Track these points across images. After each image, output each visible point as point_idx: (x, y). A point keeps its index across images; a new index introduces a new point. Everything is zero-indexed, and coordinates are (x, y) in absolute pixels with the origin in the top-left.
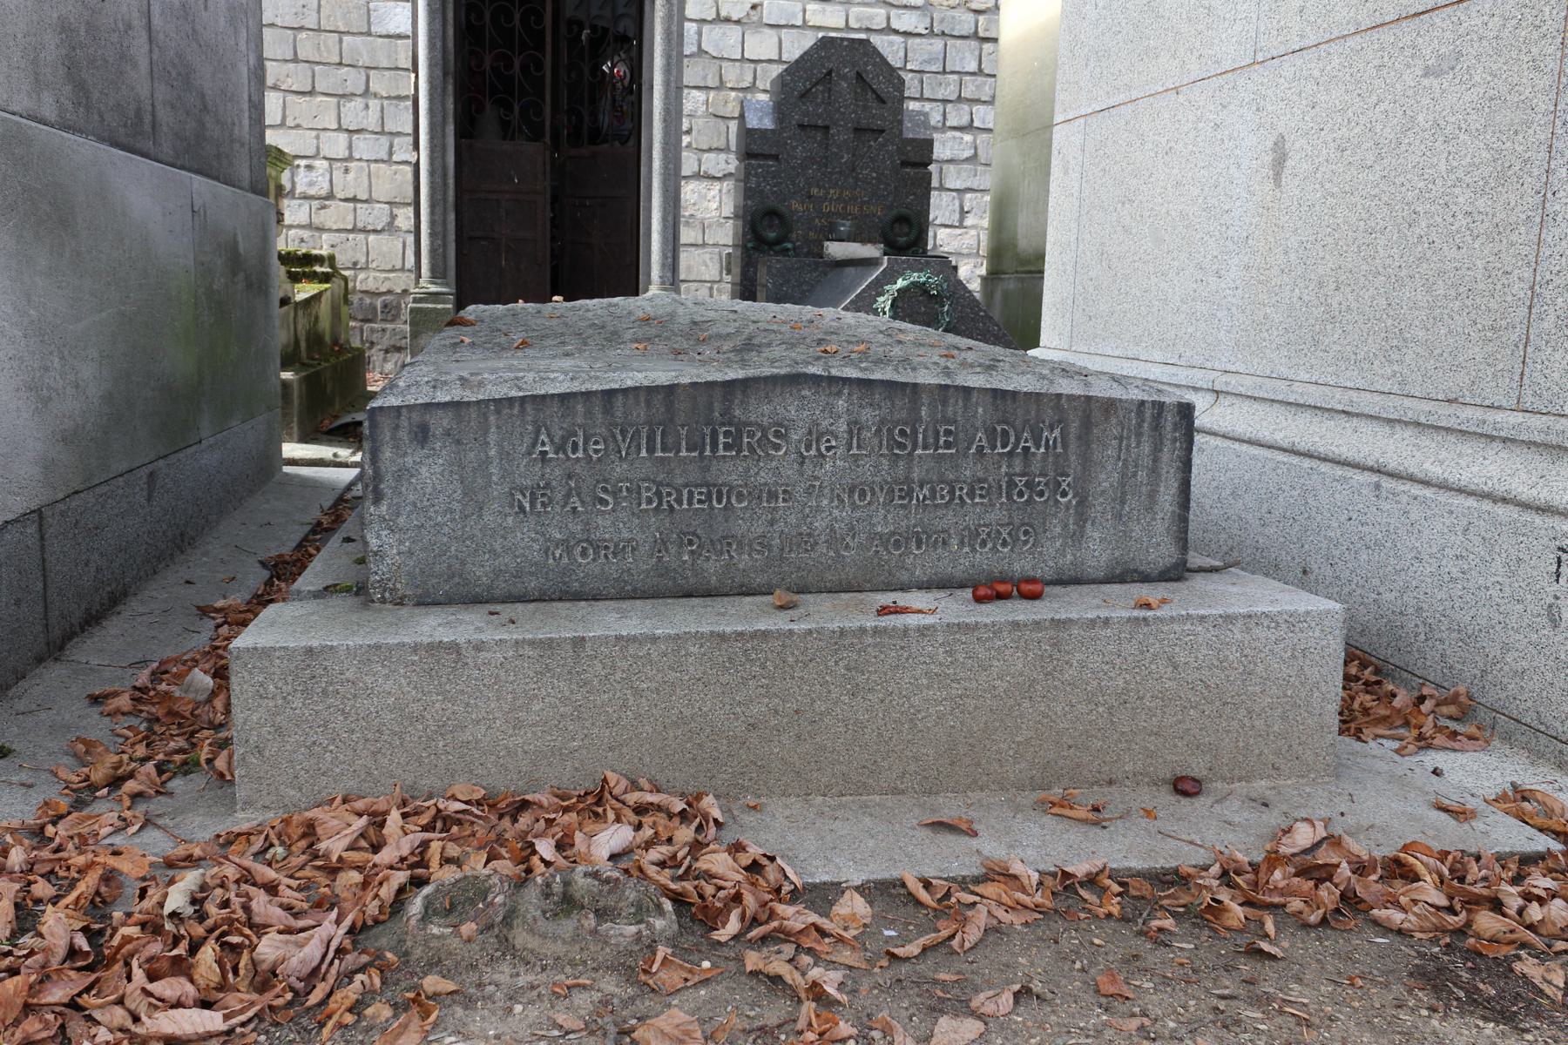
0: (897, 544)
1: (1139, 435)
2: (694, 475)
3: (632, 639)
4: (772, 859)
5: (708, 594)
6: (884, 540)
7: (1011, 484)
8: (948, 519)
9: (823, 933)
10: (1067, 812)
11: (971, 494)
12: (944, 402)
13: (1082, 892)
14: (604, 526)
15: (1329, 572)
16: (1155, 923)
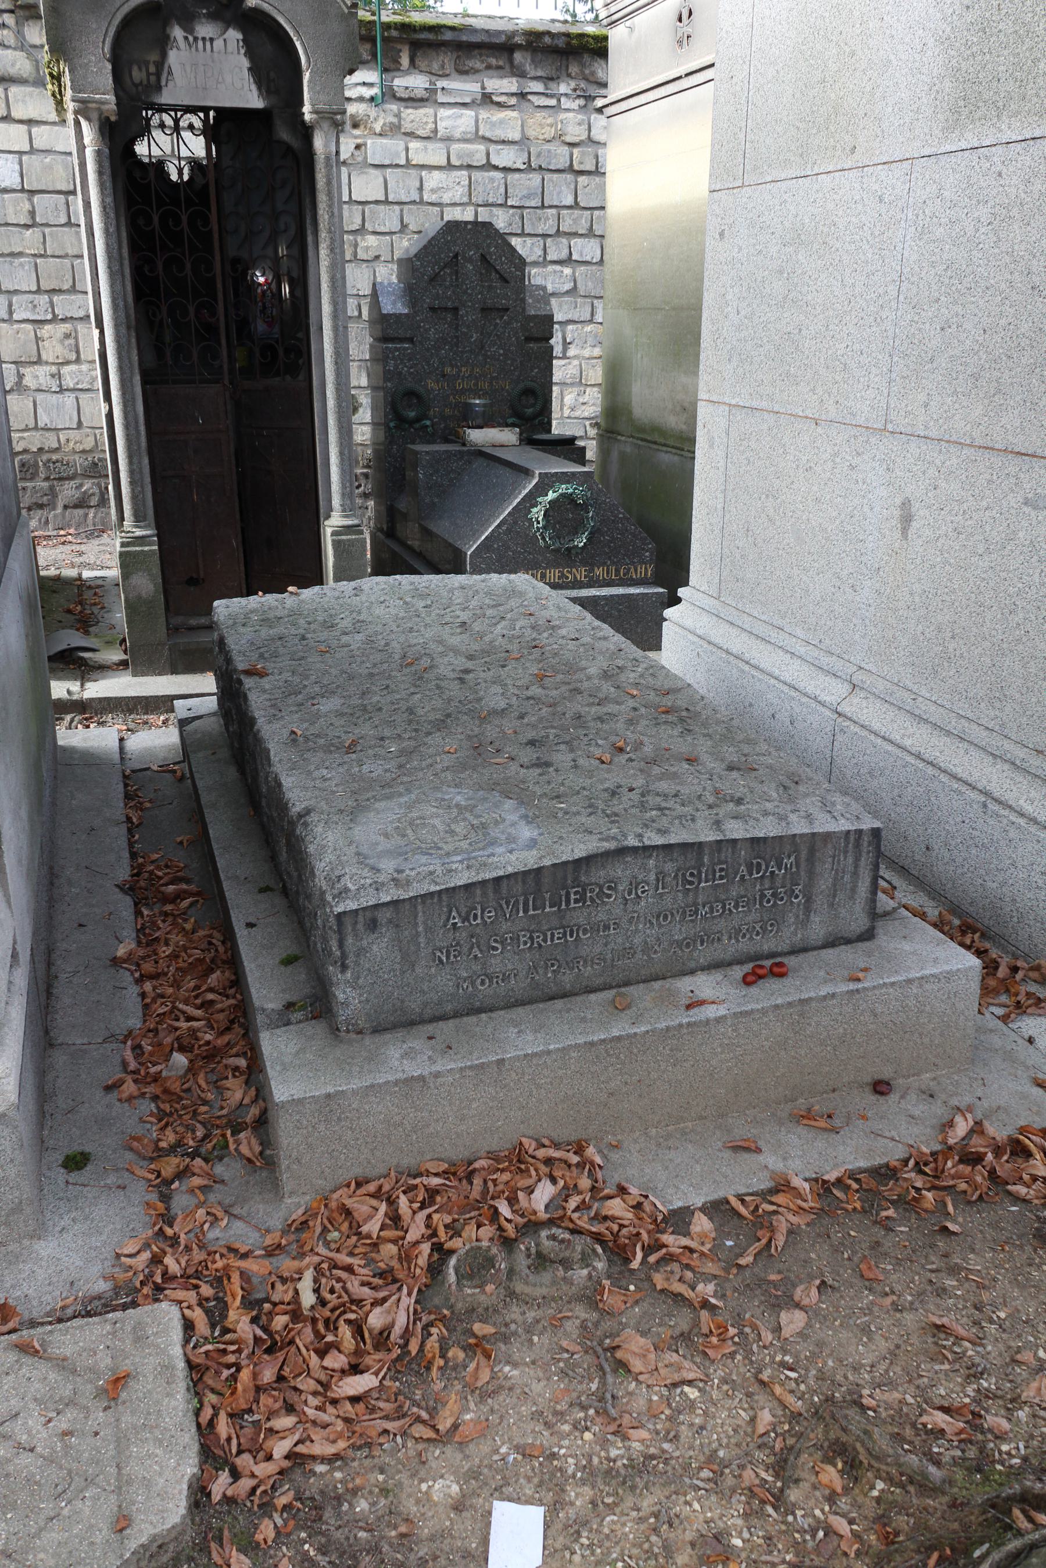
0: (688, 945)
1: (846, 852)
2: (555, 922)
3: (535, 1055)
4: (646, 1197)
5: (564, 996)
6: (679, 944)
7: (763, 896)
8: (721, 924)
9: (692, 1251)
10: (812, 1123)
11: (736, 907)
12: (719, 851)
13: (835, 1191)
14: (496, 964)
15: (947, 854)
16: (884, 1214)
